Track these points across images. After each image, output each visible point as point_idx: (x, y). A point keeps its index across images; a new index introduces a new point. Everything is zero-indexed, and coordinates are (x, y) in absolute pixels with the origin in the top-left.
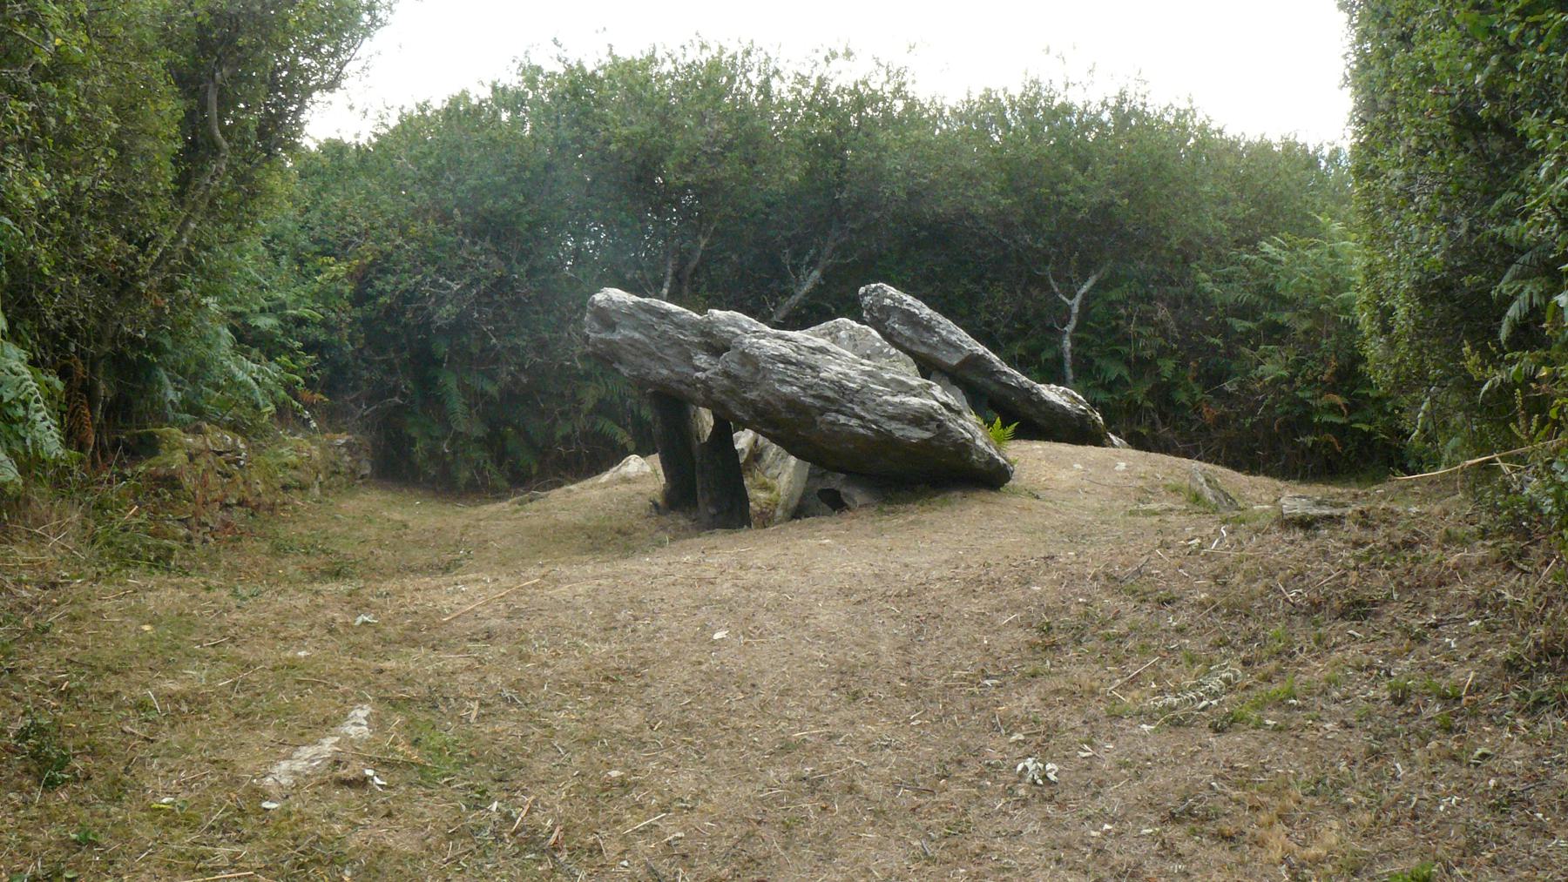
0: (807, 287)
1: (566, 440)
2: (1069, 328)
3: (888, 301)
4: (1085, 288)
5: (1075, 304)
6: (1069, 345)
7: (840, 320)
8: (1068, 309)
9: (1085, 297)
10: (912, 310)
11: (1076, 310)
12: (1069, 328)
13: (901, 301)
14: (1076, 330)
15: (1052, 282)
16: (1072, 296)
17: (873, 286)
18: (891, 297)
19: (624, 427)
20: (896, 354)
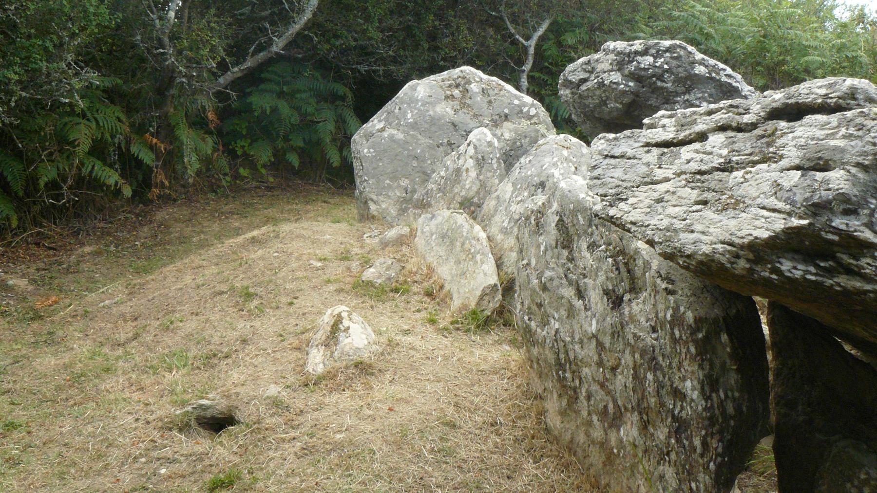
0: (307, 16)
1: (53, 185)
2: (527, 67)
3: (700, 70)
4: (540, 32)
5: (532, 43)
6: (526, 83)
7: (463, 68)
8: (525, 49)
9: (542, 39)
10: (735, 84)
11: (532, 51)
12: (527, 67)
13: (718, 71)
14: (531, 70)
15: (508, 23)
16: (528, 38)
17: (667, 43)
18: (702, 63)
19: (111, 166)
20: (536, 115)
